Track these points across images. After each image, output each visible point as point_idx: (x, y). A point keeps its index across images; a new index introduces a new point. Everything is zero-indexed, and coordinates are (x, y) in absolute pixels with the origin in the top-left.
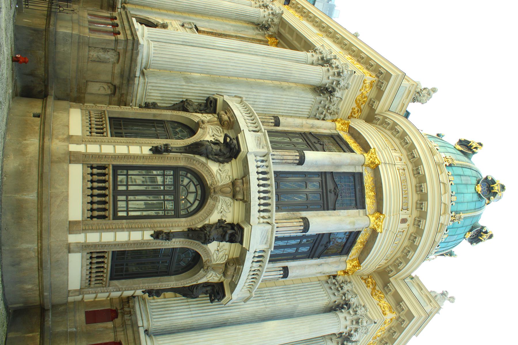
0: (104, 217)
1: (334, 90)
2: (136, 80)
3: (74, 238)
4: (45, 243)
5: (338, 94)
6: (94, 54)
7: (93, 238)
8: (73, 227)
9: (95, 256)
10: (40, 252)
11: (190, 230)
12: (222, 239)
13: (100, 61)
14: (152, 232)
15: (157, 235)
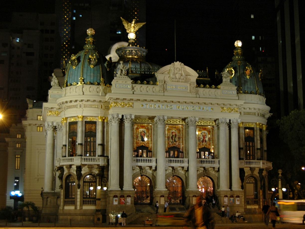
0: (75, 201)
1: (54, 126)
2: (55, 191)
3: (78, 208)
4: (78, 214)
5: (55, 124)
6: (49, 204)
7: (78, 203)
8: (76, 208)
9: (84, 202)
10: (81, 215)
11: (78, 179)
12: (81, 170)
13: (51, 202)
14: (78, 189)
15: (79, 188)
